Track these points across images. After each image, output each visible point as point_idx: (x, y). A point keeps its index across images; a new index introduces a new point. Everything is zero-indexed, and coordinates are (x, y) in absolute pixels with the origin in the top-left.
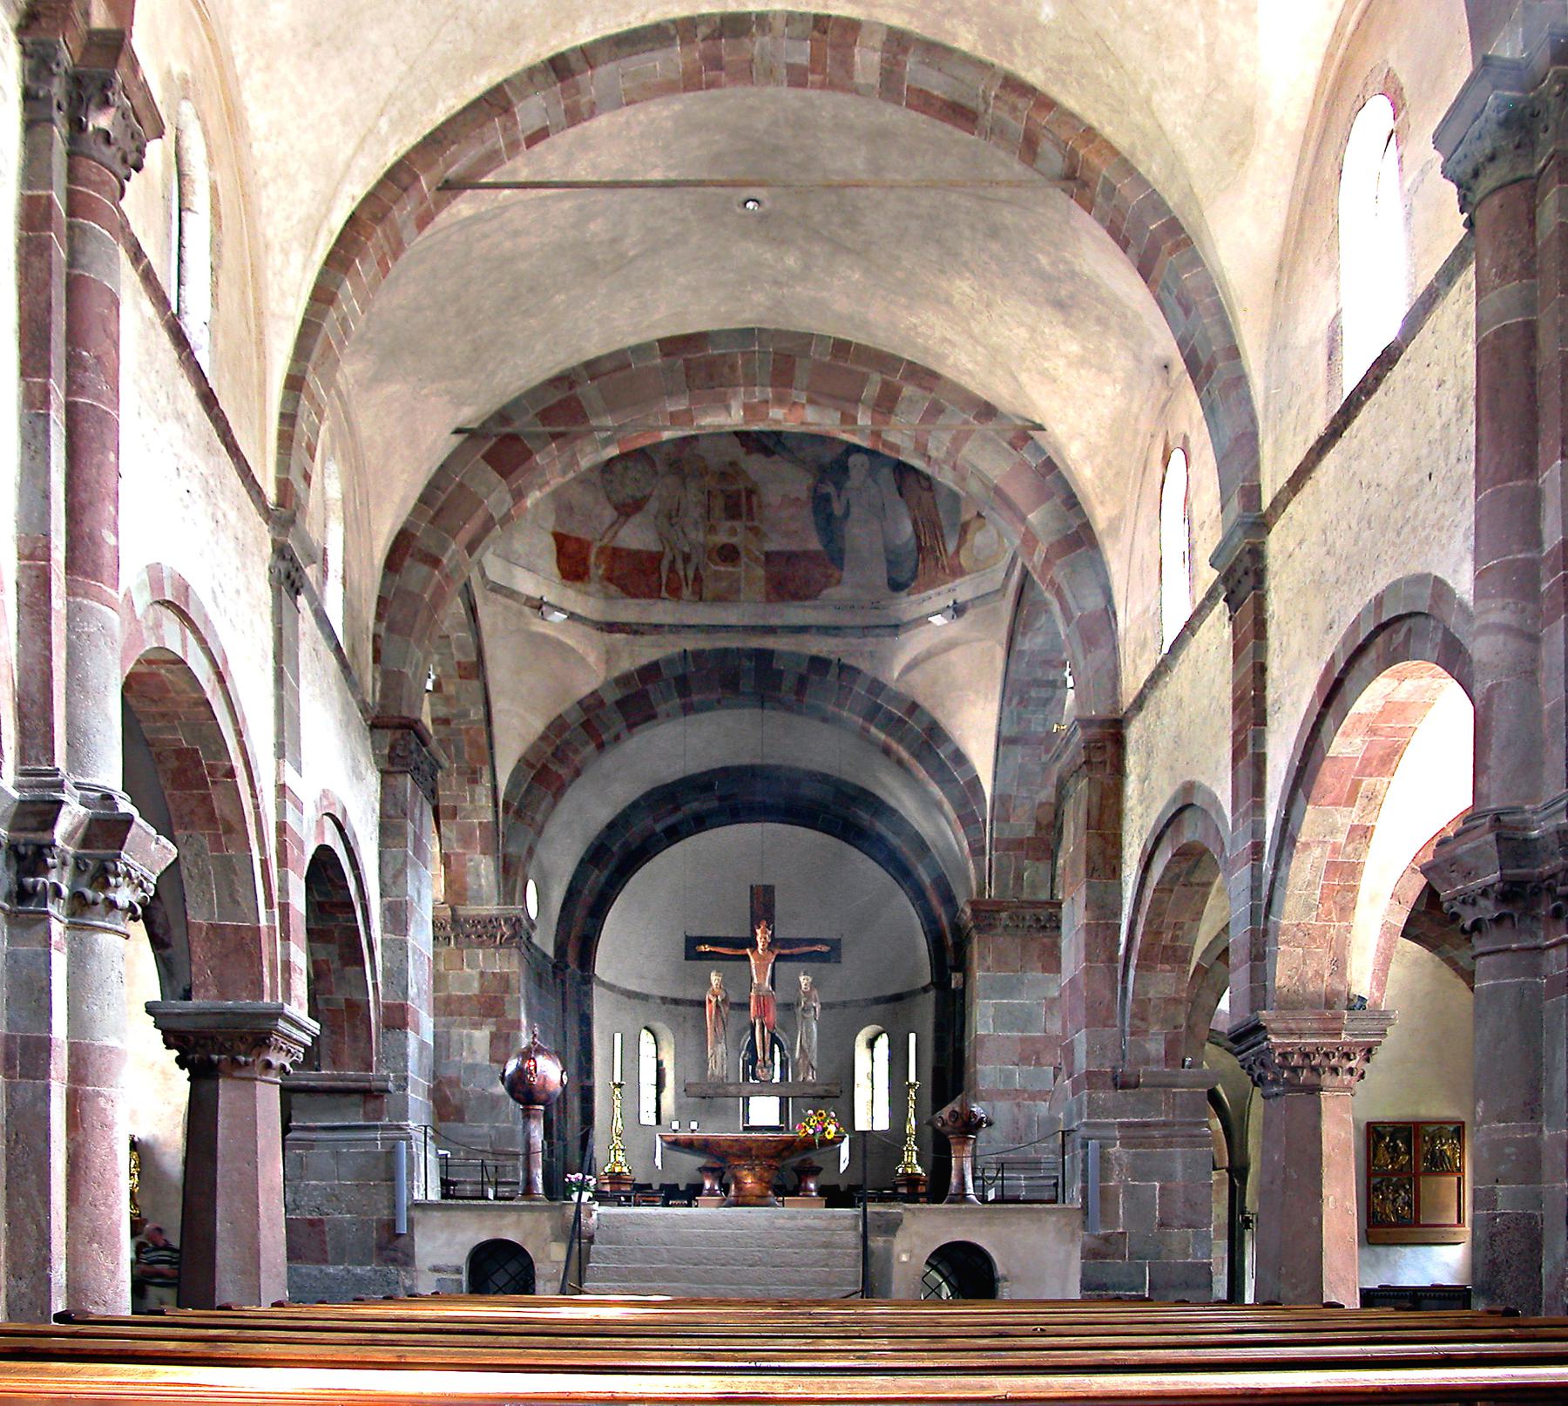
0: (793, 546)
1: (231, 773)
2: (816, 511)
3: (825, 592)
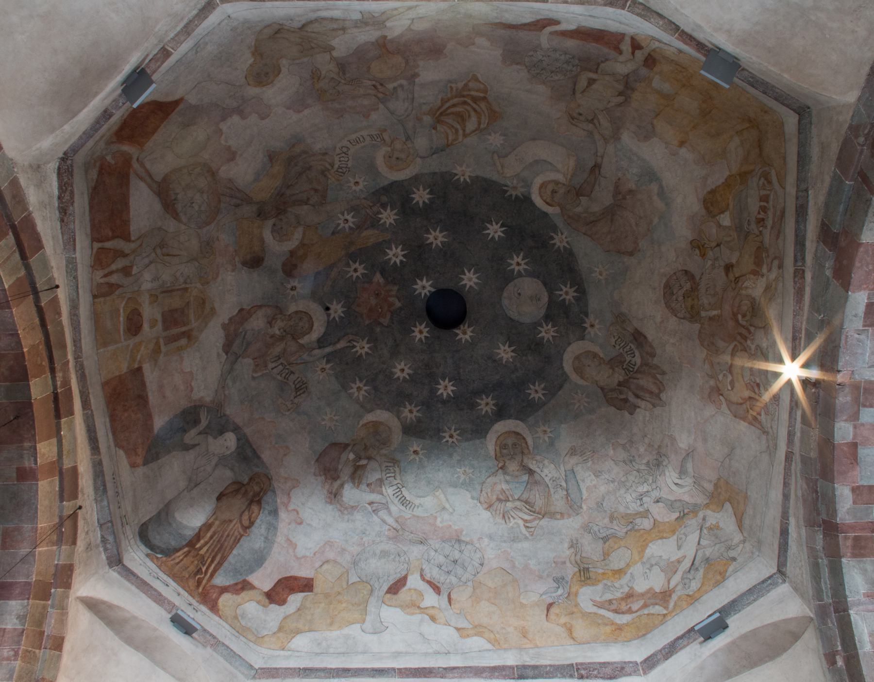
0: (153, 398)
3: (121, 453)
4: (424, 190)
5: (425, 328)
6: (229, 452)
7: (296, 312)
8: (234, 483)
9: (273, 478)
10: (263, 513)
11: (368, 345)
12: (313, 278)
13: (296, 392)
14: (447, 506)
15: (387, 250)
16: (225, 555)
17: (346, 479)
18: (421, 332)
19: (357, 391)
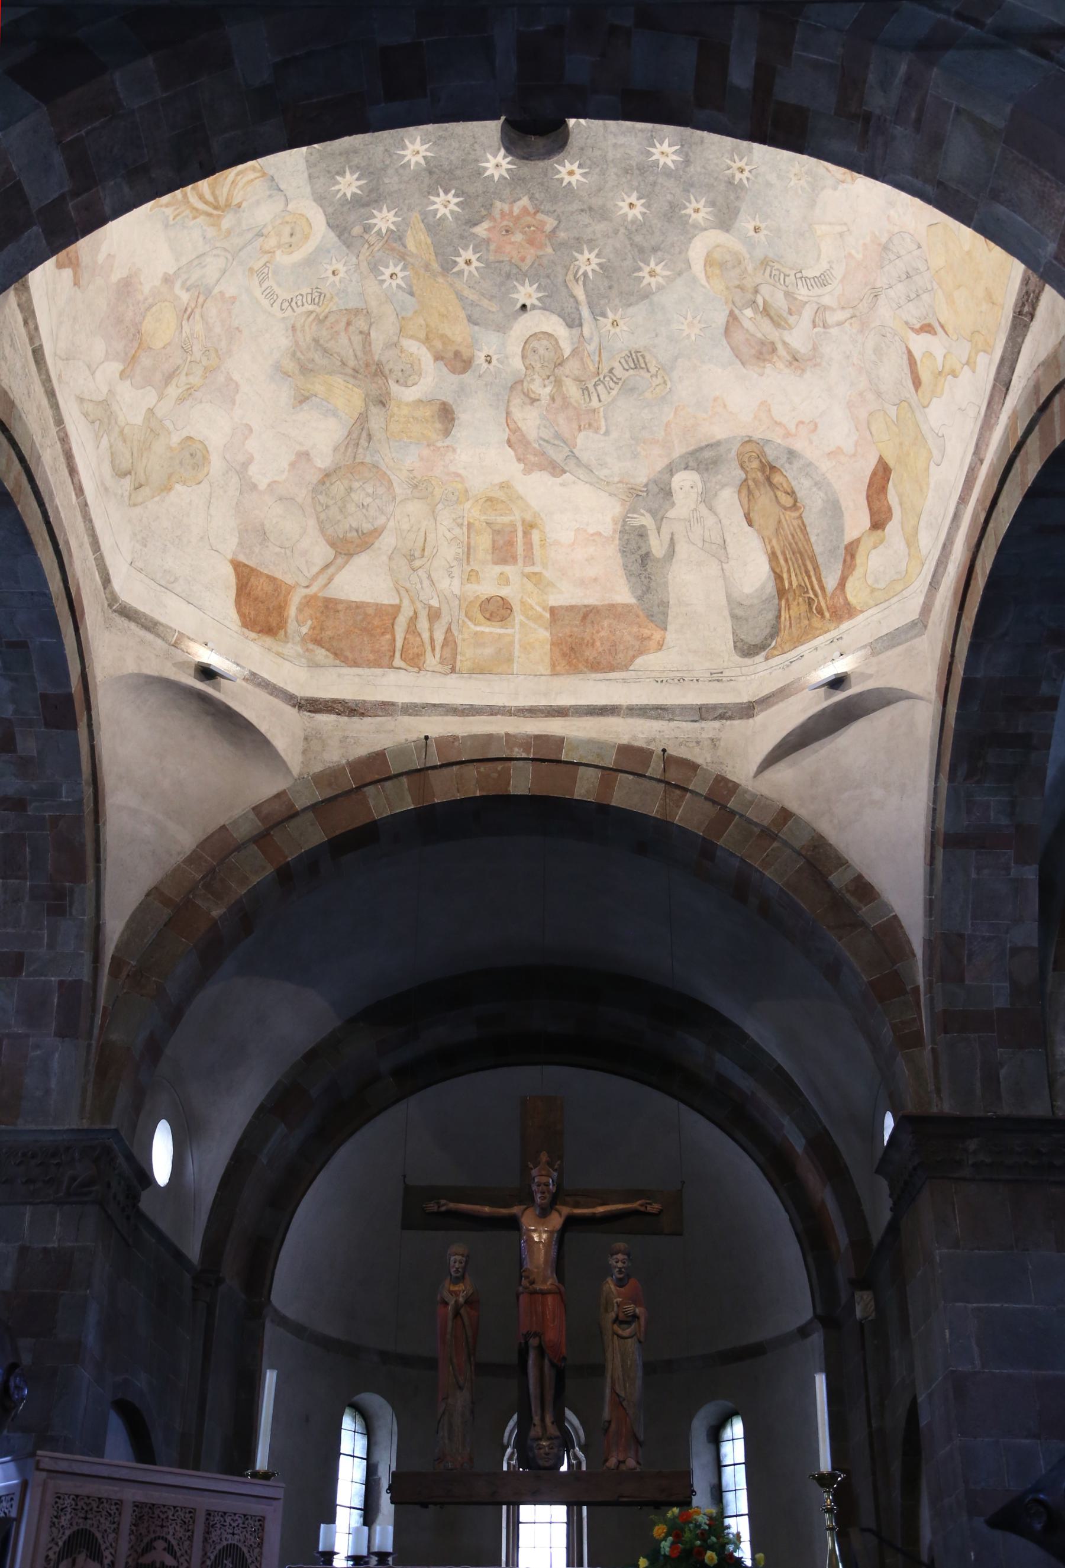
0: (592, 598)
2: (623, 552)
3: (639, 661)
4: (339, 183)
5: (565, 167)
6: (700, 485)
7: (524, 357)
8: (739, 492)
9: (750, 435)
10: (786, 471)
11: (586, 252)
12: (476, 328)
13: (642, 368)
14: (839, 229)
15: (438, 217)
16: (811, 554)
17: (777, 334)
18: (571, 173)
19: (655, 276)
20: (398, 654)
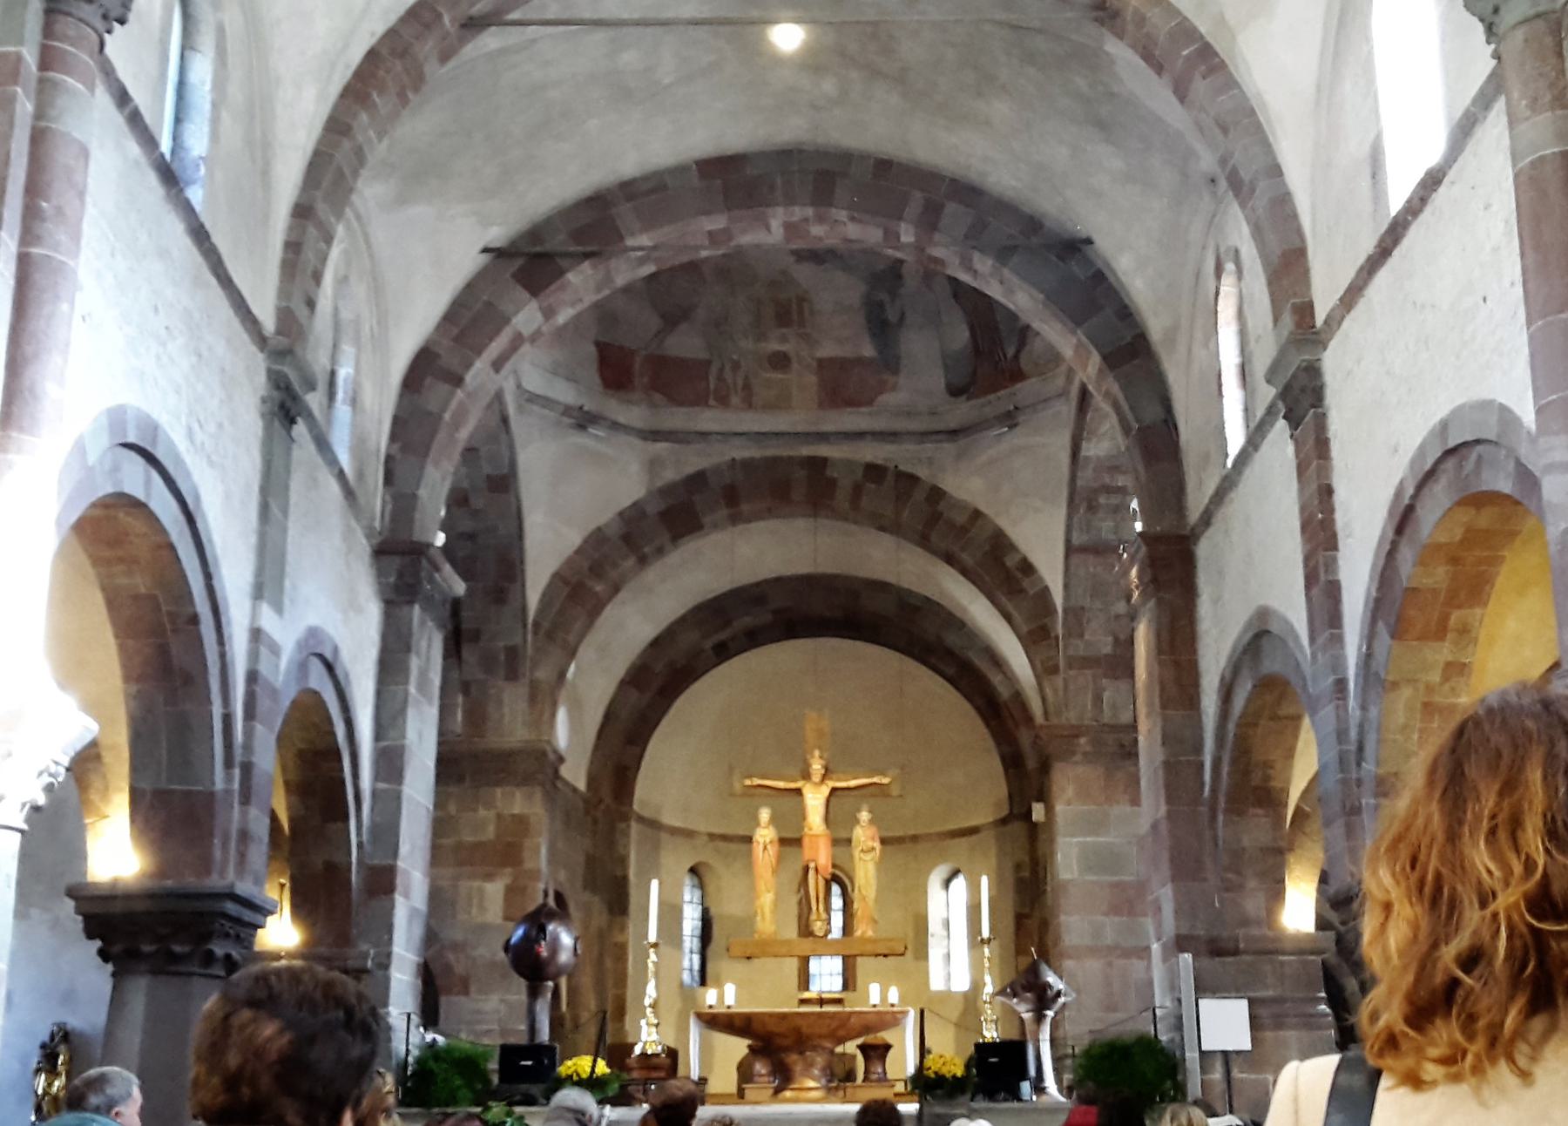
1: (194, 620)
20: (712, 397)
